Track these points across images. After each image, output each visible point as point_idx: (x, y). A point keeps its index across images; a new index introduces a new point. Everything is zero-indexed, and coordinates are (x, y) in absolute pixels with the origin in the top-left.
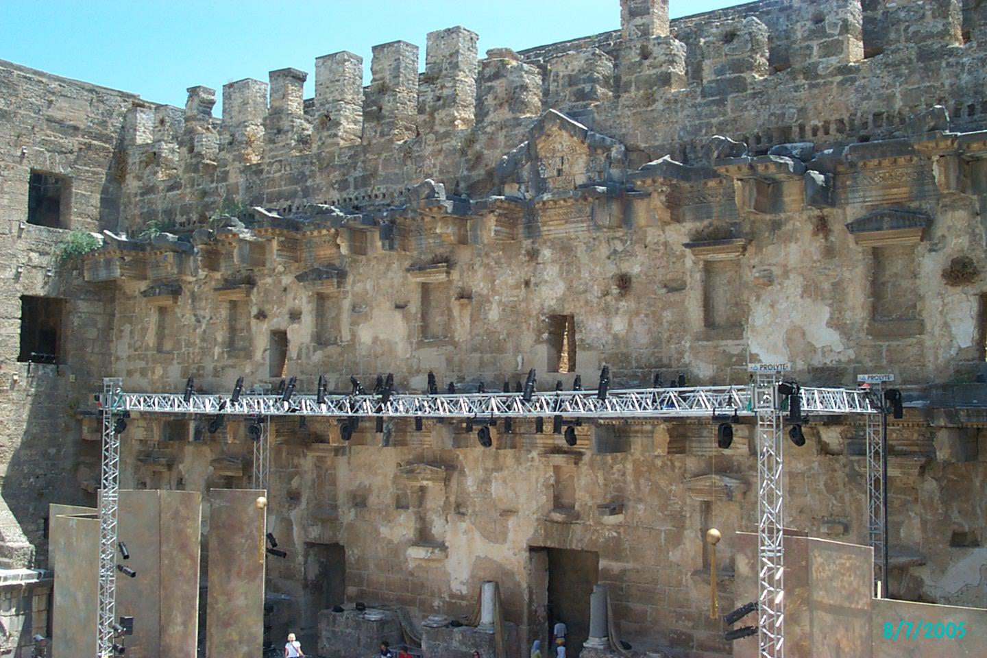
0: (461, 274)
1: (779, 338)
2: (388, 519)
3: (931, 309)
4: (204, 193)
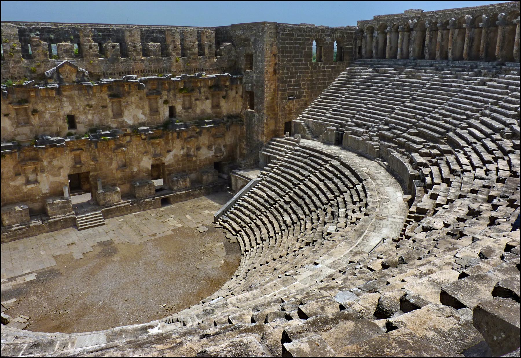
0: (33, 104)
1: (131, 117)
2: (13, 179)
3: (161, 110)
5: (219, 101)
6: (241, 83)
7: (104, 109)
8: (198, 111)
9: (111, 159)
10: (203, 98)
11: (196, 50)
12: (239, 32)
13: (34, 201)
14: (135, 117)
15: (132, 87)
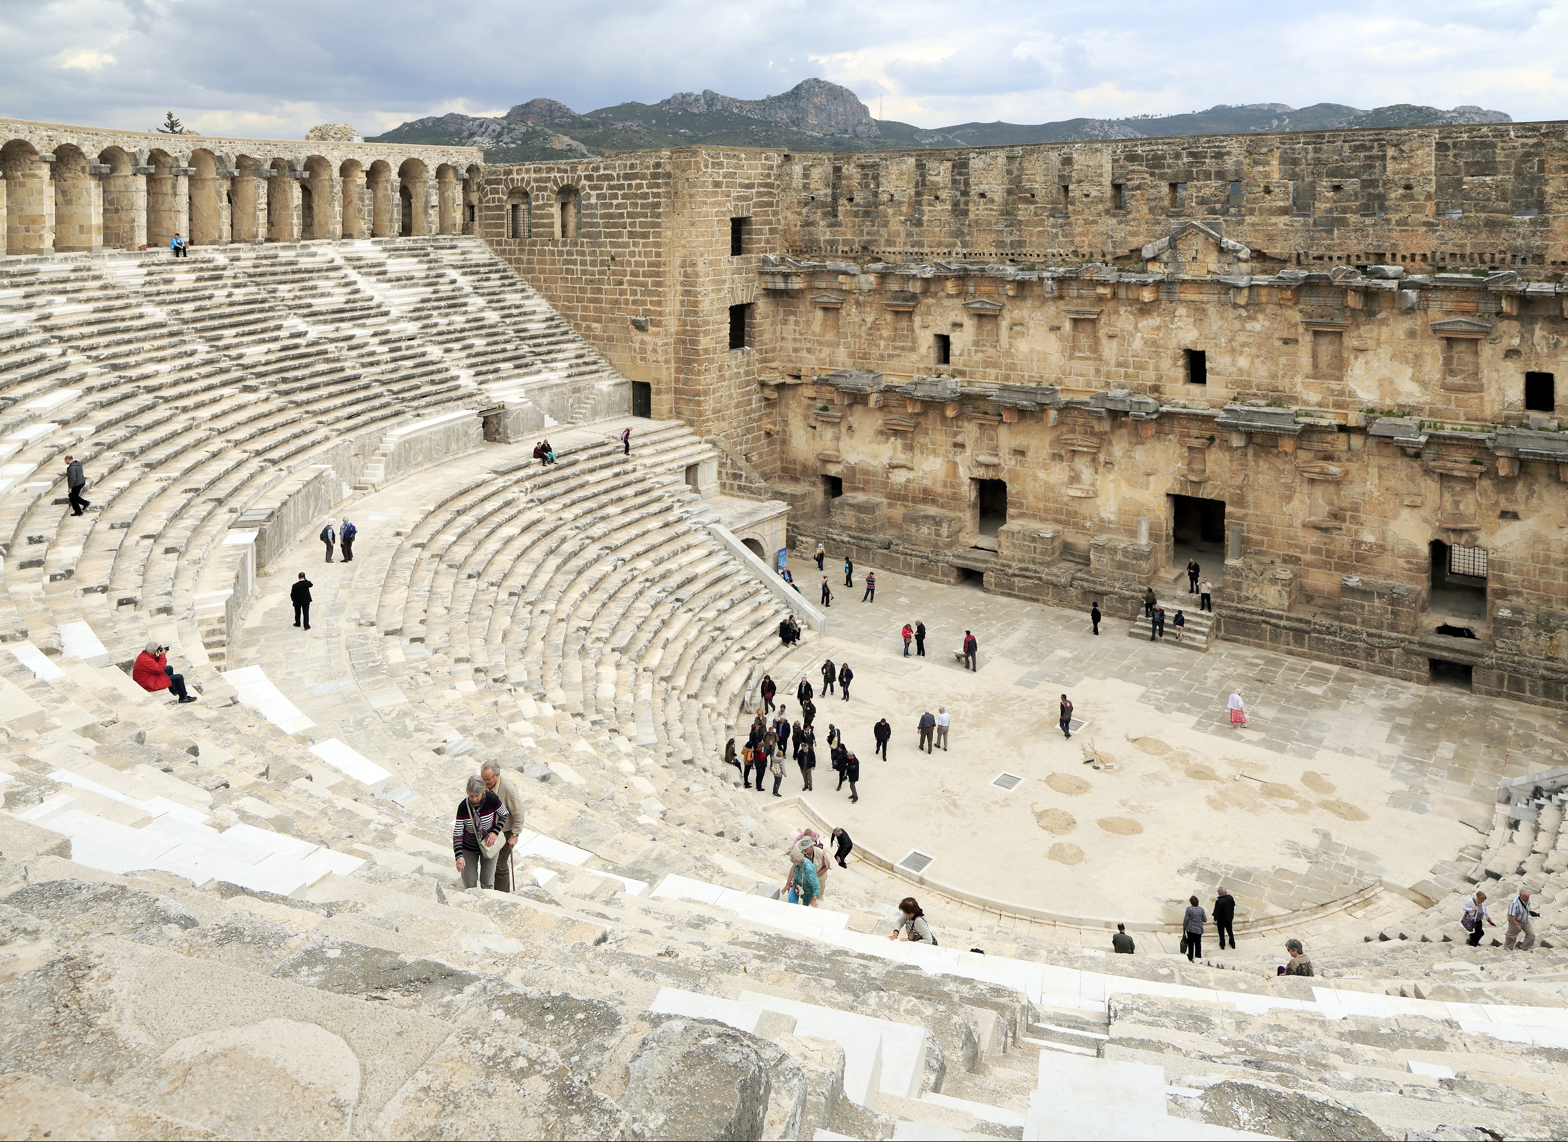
7: (1286, 348)
13: (1082, 529)
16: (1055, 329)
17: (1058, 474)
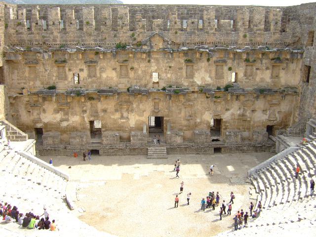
2: (113, 114)
4: (44, 37)
5: (279, 72)
6: (302, 57)
8: (258, 79)
9: (180, 110)
10: (264, 68)
11: (263, 27)
12: (306, 11)
13: (124, 131)
14: (203, 79)
15: (204, 55)
16: (114, 69)
17: (117, 116)
